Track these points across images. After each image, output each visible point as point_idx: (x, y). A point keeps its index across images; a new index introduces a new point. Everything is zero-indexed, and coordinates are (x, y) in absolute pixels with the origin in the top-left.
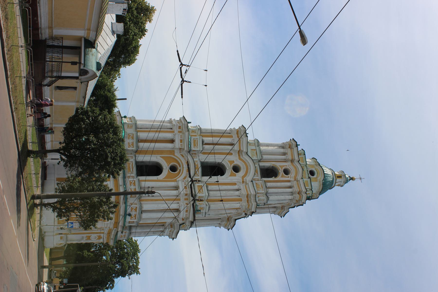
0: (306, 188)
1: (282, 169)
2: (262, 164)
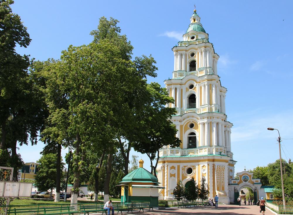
1: (190, 57)
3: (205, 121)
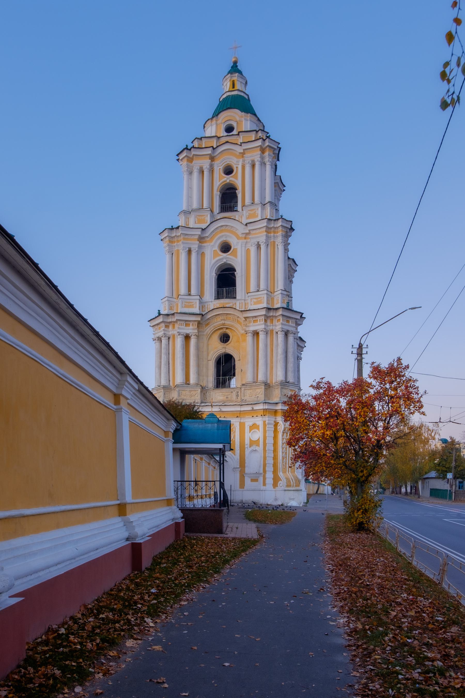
0: (253, 139)
3: (259, 326)
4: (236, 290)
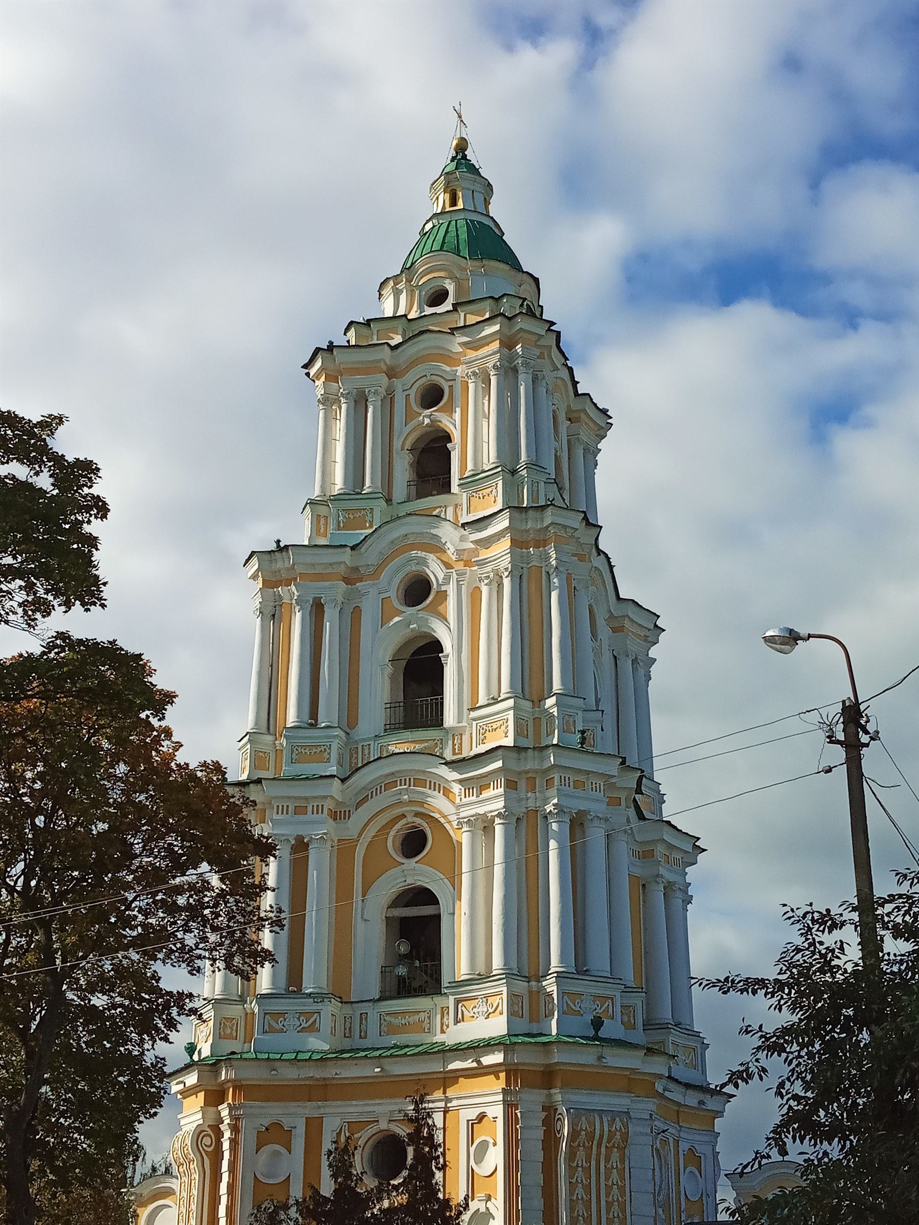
2: (400, 490)
4: (442, 703)
